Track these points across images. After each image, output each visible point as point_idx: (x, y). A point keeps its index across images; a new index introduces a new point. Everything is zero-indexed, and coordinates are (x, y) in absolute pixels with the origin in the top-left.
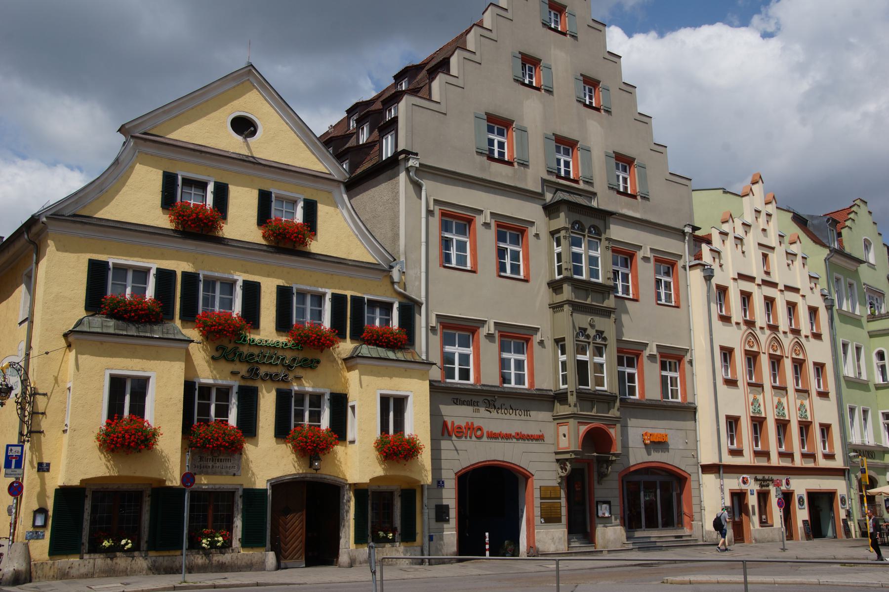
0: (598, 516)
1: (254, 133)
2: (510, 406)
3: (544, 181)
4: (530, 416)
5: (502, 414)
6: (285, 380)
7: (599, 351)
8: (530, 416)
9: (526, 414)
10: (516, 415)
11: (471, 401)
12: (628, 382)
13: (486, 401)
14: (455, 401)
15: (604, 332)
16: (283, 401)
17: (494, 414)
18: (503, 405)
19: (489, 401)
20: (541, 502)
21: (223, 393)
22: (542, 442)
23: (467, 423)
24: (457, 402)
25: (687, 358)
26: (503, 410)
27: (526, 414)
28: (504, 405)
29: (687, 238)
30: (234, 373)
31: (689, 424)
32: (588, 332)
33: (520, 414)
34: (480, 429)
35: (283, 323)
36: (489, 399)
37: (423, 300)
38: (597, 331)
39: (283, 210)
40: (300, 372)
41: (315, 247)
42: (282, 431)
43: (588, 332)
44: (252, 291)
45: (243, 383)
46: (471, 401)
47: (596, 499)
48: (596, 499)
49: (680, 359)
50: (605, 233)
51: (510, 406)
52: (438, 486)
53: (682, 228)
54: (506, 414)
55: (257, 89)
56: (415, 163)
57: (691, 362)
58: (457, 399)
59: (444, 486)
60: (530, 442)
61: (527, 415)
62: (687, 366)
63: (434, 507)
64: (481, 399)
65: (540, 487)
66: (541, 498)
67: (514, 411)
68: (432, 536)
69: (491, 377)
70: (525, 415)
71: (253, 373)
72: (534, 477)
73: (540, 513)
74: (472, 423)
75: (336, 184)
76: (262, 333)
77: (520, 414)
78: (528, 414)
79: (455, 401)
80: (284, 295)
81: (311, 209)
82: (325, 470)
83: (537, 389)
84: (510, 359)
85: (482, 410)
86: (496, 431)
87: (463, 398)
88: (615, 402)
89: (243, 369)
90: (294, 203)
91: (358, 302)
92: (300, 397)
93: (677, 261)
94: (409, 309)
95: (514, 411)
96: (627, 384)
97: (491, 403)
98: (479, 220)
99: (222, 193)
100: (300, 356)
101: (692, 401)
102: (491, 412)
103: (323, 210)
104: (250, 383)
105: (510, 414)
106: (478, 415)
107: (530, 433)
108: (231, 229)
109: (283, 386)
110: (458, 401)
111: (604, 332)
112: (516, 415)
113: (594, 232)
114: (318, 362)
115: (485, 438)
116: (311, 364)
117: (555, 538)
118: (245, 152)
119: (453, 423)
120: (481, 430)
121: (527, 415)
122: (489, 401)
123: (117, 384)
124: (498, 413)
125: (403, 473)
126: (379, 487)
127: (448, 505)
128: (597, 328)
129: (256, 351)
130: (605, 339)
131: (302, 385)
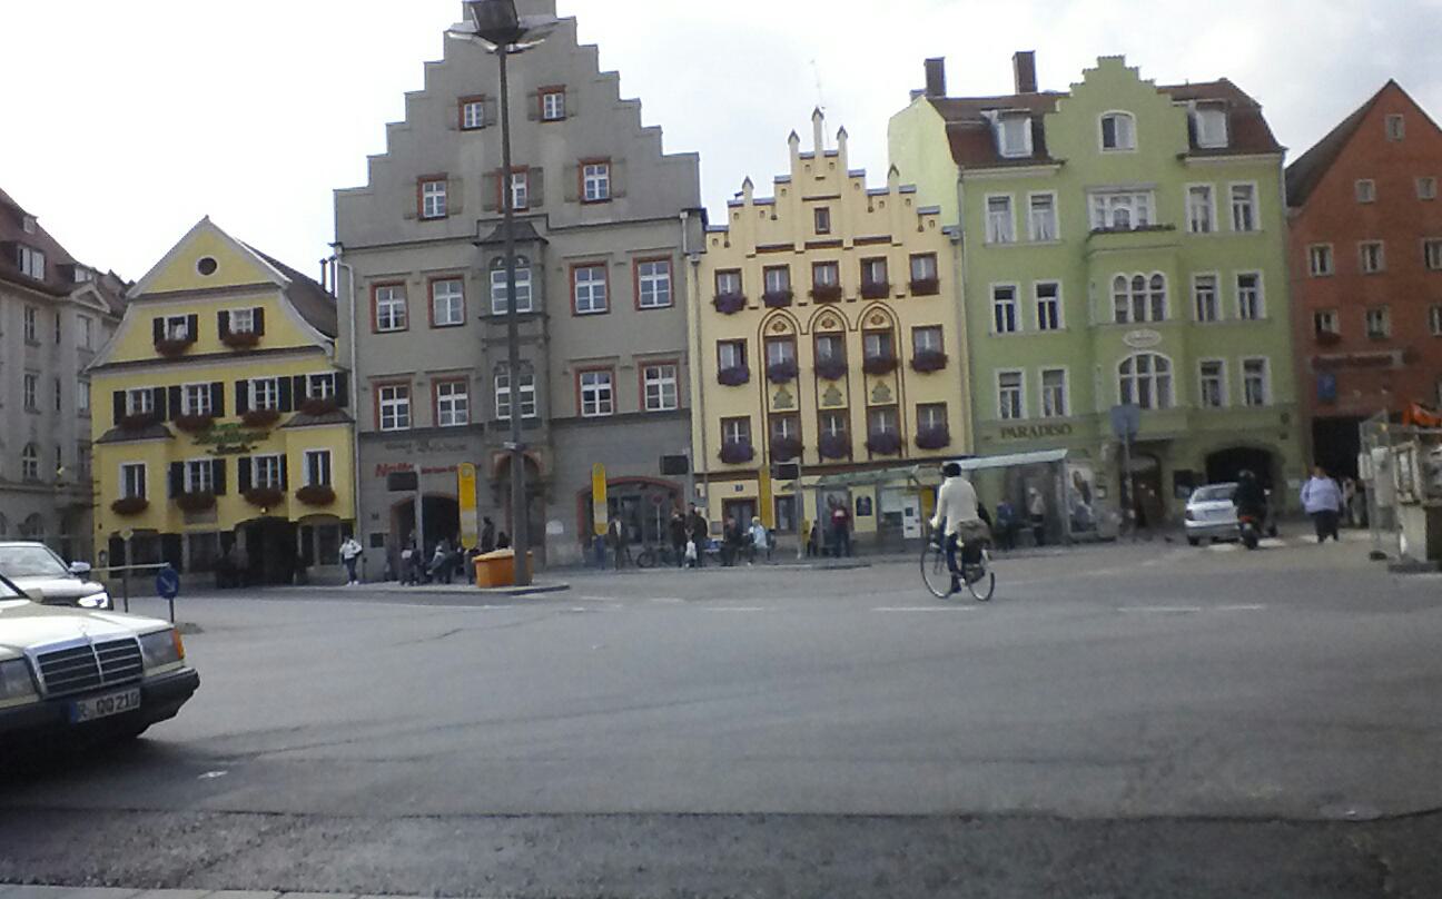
1: (212, 271)
3: (479, 221)
6: (243, 449)
12: (393, 426)
16: (245, 466)
21: (207, 464)
30: (209, 452)
40: (254, 444)
41: (266, 343)
44: (218, 388)
45: (216, 457)
53: (675, 215)
69: (422, 419)
71: (222, 450)
80: (242, 387)
82: (277, 513)
86: (430, 467)
89: (214, 448)
91: (300, 380)
92: (262, 462)
94: (342, 378)
96: (396, 428)
99: (193, 320)
100: (254, 431)
104: (221, 457)
108: (201, 347)
109: (245, 455)
114: (268, 434)
116: (265, 436)
119: (386, 465)
123: (129, 470)
125: (327, 511)
129: (222, 433)
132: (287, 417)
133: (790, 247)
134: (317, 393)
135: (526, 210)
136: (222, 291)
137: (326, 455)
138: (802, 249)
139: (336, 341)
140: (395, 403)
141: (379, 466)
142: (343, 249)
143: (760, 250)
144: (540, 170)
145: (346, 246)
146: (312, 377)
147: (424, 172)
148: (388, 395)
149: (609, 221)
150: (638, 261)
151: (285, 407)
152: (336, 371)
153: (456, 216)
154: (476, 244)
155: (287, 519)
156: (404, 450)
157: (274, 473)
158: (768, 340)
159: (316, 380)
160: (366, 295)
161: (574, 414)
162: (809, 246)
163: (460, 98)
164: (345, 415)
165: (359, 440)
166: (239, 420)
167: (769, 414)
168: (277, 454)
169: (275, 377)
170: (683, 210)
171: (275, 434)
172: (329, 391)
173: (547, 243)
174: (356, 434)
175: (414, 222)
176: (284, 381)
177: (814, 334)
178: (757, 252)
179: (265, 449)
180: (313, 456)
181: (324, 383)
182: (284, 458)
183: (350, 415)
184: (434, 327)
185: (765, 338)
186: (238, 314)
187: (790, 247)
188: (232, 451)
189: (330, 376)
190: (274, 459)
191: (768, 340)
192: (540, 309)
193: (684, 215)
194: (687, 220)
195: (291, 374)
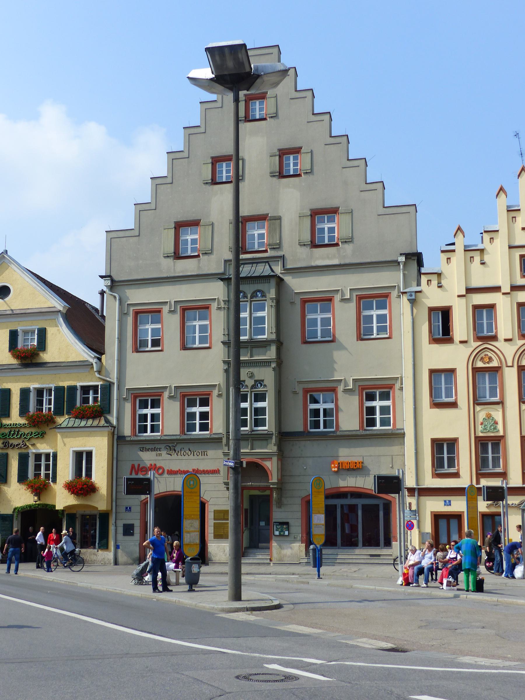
0: (274, 535)
2: (189, 449)
4: (207, 455)
5: (181, 455)
7: (259, 397)
8: (207, 455)
9: (203, 454)
10: (194, 455)
11: (155, 448)
13: (167, 447)
14: (142, 450)
15: (264, 380)
16: (23, 460)
17: (175, 456)
18: (182, 449)
19: (170, 447)
20: (214, 523)
22: (219, 475)
23: (151, 465)
24: (143, 450)
25: (397, 386)
26: (182, 452)
27: (203, 454)
28: (183, 449)
29: (401, 266)
31: (395, 449)
32: (246, 383)
33: (198, 454)
34: (160, 468)
35: (24, 410)
36: (170, 445)
37: (115, 381)
38: (256, 381)
39: (31, 338)
41: (47, 357)
42: (22, 478)
43: (246, 383)
46: (155, 448)
47: (274, 521)
48: (274, 521)
49: (391, 387)
50: (269, 293)
51: (189, 449)
52: (126, 510)
54: (184, 456)
55: (14, 264)
56: (107, 283)
57: (401, 389)
58: (143, 448)
59: (130, 511)
60: (207, 475)
61: (204, 455)
62: (397, 392)
63: (123, 525)
64: (162, 446)
65: (214, 510)
66: (215, 519)
67: (192, 453)
68: (119, 545)
70: (202, 455)
72: (209, 503)
73: (213, 531)
74: (155, 465)
75: (56, 313)
76: (13, 419)
77: (198, 454)
78: (205, 454)
79: (142, 450)
80: (25, 393)
81: (42, 334)
82: (47, 500)
83: (214, 434)
84: (196, 413)
85: (164, 453)
86: (175, 469)
87: (148, 446)
88: (271, 438)
90: (33, 332)
91: (72, 389)
92: (38, 457)
93: (390, 293)
94: (108, 388)
95: (192, 453)
97: (171, 448)
98: (165, 309)
100: (34, 430)
101: (402, 427)
102: (171, 455)
103: (51, 332)
104: (5, 451)
105: (189, 456)
106: (160, 458)
107: (206, 469)
109: (23, 451)
110: (144, 449)
111: (264, 380)
112: (194, 455)
113: (260, 295)
115: (166, 475)
116: (42, 435)
117: (226, 551)
118: (5, 308)
119: (139, 465)
120: (161, 468)
121: (204, 455)
122: (170, 447)
124: (178, 455)
126: (84, 511)
127: (134, 524)
128: (256, 379)
129: (7, 431)
130: (265, 386)
131: (37, 449)
132: (60, 420)
133: (496, 289)
134: (85, 400)
135: (266, 251)
136: (14, 315)
137: (89, 454)
138: (508, 290)
139: (103, 357)
140: (149, 411)
141: (133, 466)
142: (113, 281)
143: (470, 290)
144: (279, 218)
145: (116, 278)
146: (82, 387)
147: (181, 218)
148: (144, 405)
149: (336, 262)
150: (360, 298)
151: (59, 411)
152: (101, 383)
153: (206, 257)
154: (222, 280)
155: (55, 506)
156: (154, 453)
157: (47, 468)
158: (476, 370)
159: (85, 390)
160: (130, 320)
161: (301, 429)
162: (515, 288)
163: (212, 158)
164: (107, 421)
165: (117, 440)
166: (23, 421)
167: (476, 438)
168: (51, 451)
169: (53, 386)
170: (401, 254)
171: (50, 433)
172: (95, 399)
173: (282, 280)
174: (116, 437)
175: (170, 261)
176: (59, 390)
177: (519, 367)
178: (467, 293)
179: (43, 448)
180: (78, 455)
181: (91, 392)
182: (55, 456)
183: (112, 422)
184: (184, 347)
185: (473, 369)
186: (26, 332)
187: (496, 289)
188: (13, 446)
189: (97, 386)
190: (47, 455)
191: (476, 370)
192: (274, 337)
193: (402, 259)
194: (405, 264)
195: (66, 384)
